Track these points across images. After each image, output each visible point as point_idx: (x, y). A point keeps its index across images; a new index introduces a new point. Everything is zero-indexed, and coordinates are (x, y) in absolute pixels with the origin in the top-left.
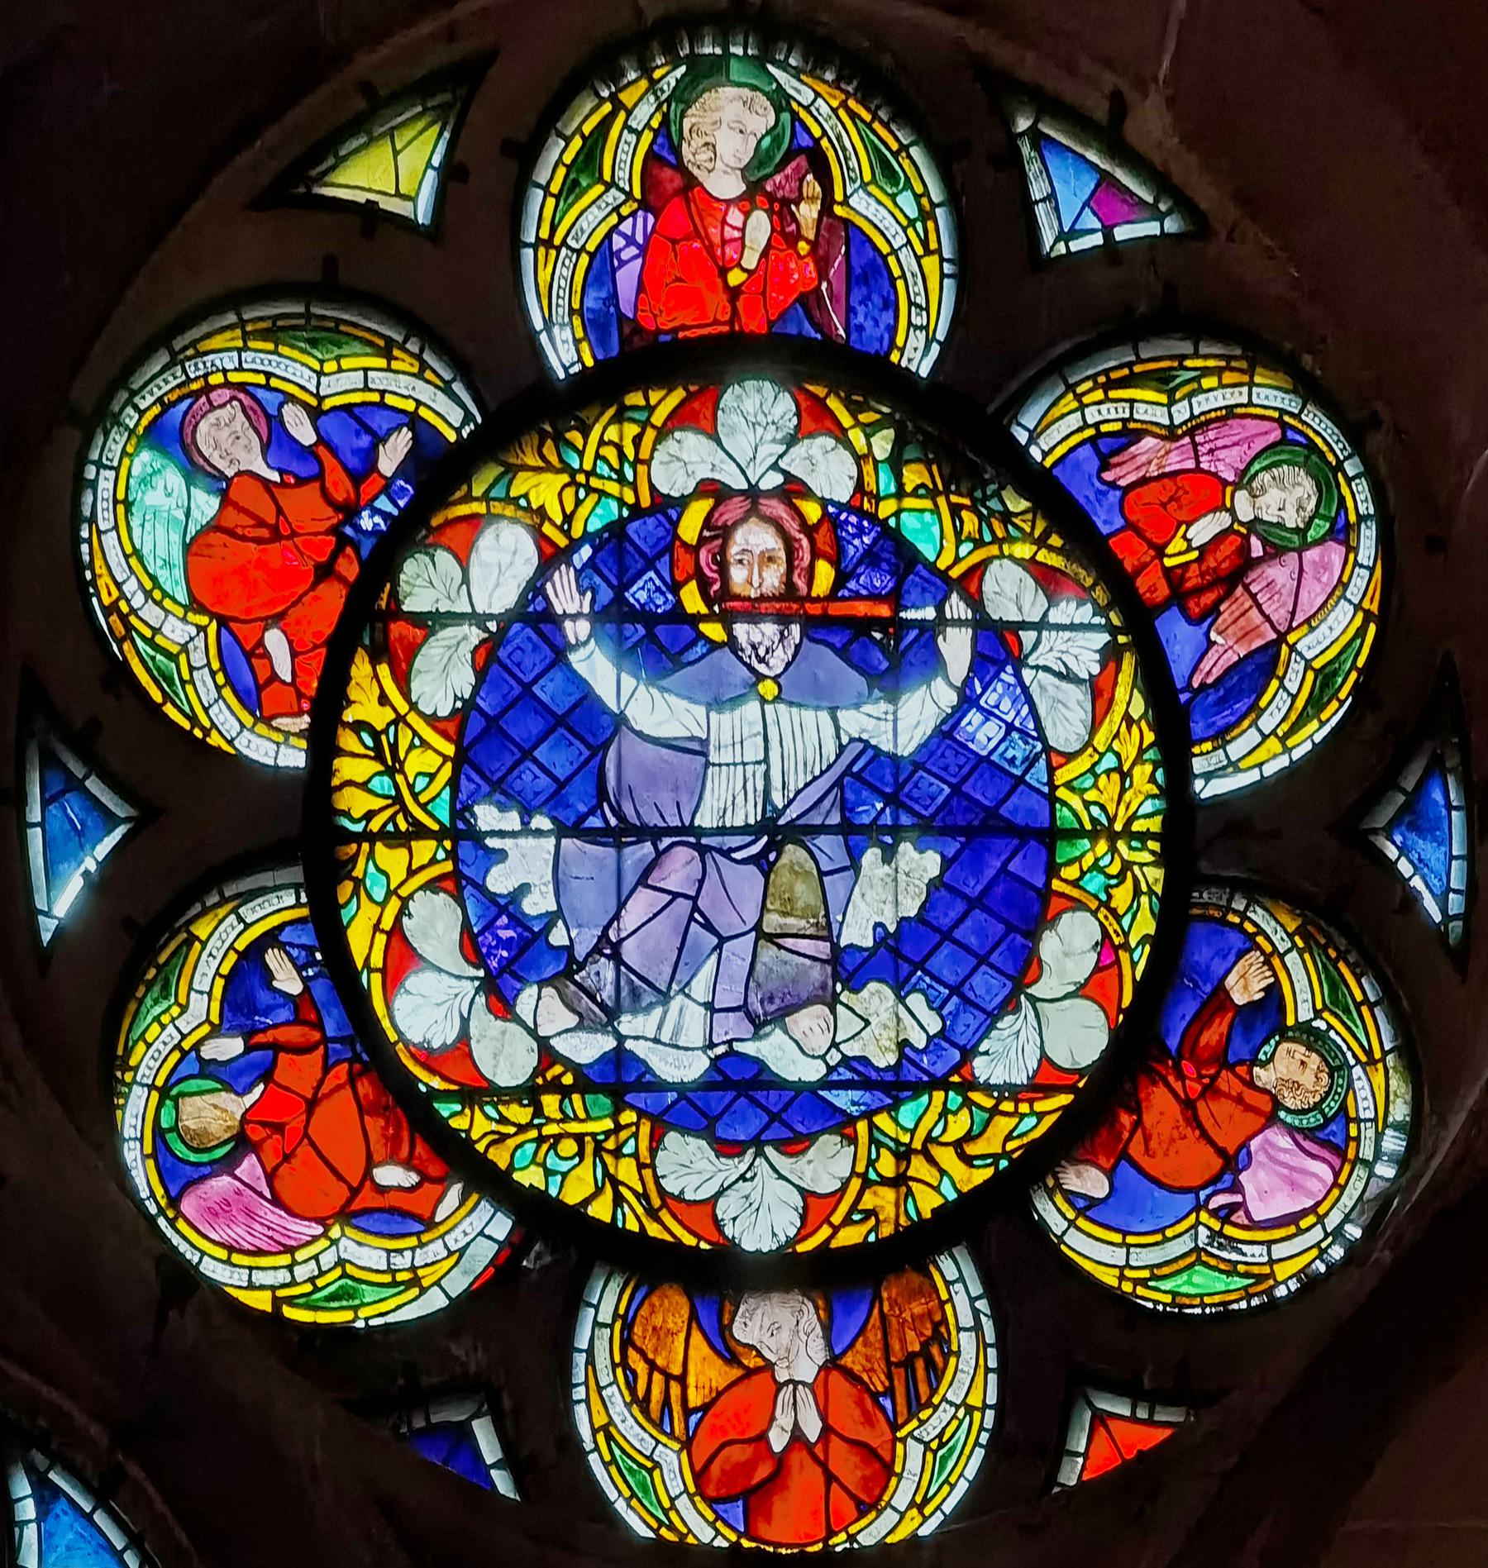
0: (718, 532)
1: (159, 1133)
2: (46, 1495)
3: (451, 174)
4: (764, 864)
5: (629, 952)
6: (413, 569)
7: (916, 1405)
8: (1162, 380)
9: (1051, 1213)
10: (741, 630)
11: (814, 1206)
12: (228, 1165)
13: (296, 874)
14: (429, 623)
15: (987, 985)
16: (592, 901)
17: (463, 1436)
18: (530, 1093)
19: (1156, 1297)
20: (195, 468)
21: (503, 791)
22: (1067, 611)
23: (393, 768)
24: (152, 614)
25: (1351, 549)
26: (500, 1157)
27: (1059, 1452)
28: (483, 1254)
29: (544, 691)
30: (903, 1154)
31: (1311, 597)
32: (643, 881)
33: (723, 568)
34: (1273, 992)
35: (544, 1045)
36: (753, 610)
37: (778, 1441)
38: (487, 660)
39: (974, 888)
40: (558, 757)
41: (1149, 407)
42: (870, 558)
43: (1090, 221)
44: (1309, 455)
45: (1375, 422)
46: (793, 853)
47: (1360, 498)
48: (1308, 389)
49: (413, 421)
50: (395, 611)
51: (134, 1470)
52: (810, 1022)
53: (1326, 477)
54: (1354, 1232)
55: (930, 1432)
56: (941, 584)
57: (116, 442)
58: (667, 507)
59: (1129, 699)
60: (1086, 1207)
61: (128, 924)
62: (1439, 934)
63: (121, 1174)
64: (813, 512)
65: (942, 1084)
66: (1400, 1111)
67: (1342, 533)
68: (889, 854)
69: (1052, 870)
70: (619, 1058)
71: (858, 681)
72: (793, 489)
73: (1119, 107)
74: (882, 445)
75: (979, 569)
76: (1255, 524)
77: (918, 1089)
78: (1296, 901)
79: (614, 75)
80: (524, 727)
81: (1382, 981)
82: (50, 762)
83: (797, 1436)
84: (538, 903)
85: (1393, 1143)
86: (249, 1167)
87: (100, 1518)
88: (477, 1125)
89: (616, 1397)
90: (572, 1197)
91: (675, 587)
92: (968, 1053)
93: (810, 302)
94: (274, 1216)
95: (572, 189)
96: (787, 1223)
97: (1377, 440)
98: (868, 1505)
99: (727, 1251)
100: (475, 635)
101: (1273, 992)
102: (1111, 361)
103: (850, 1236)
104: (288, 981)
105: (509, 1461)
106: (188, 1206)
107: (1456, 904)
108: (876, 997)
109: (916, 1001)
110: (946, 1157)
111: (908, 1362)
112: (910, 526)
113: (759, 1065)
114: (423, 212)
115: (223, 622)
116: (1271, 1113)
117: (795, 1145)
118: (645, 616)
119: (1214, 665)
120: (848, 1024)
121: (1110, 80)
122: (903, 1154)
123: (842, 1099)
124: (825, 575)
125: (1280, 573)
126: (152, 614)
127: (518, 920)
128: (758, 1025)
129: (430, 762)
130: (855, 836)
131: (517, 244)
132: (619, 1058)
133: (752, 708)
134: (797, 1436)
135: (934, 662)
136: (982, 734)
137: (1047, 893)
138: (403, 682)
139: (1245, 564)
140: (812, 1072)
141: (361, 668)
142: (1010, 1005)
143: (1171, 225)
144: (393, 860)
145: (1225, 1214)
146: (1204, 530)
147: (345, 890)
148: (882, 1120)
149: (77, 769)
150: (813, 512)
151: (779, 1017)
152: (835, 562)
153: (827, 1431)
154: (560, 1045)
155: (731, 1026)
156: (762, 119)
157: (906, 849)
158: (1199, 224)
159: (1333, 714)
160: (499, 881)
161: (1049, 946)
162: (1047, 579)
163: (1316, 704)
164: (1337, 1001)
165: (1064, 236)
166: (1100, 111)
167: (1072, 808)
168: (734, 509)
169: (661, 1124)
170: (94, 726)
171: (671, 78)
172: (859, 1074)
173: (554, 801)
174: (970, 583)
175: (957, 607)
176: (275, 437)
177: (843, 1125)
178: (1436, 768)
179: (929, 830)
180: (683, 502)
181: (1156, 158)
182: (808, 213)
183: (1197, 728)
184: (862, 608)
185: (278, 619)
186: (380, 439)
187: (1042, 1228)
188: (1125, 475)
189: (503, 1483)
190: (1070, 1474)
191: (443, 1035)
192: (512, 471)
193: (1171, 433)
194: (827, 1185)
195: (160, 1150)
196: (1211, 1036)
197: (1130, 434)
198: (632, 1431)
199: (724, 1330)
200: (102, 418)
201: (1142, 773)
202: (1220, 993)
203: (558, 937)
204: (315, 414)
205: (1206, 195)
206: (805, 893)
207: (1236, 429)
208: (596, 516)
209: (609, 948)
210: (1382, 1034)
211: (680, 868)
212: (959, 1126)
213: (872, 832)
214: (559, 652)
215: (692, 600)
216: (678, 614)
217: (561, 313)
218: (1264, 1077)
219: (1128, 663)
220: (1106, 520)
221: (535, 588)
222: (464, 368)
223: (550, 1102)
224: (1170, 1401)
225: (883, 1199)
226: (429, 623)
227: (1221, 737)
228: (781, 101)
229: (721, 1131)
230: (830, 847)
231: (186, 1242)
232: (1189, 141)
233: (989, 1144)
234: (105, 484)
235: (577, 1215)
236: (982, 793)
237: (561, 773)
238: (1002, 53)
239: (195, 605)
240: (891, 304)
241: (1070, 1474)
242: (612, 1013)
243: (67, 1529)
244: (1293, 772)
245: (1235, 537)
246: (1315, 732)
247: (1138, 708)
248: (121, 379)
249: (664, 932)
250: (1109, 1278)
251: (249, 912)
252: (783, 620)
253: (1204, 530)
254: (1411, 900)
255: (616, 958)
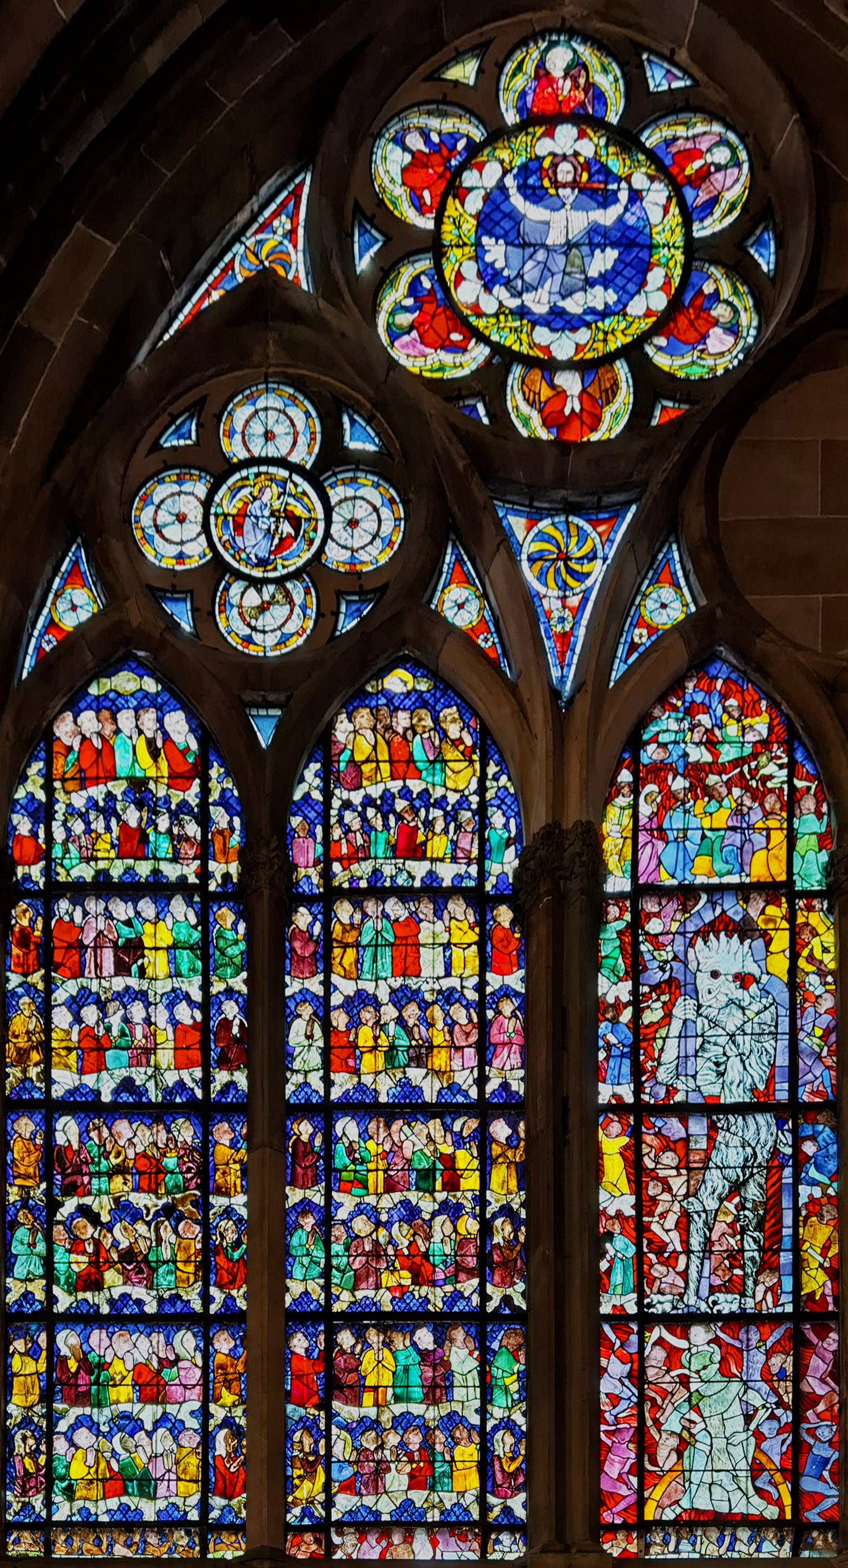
0: (554, 166)
1: (388, 325)
2: (353, 422)
3: (480, 71)
4: (566, 254)
5: (526, 277)
6: (466, 175)
7: (608, 402)
8: (685, 124)
9: (650, 350)
10: (561, 191)
11: (579, 348)
12: (409, 333)
13: (430, 255)
14: (470, 190)
15: (631, 287)
16: (516, 263)
17: (474, 408)
18: (496, 315)
19: (681, 374)
20: (405, 149)
21: (491, 234)
22: (657, 186)
23: (459, 227)
24: (391, 186)
25: (740, 170)
26: (487, 333)
27: (651, 416)
28: (481, 359)
29: (502, 207)
30: (606, 333)
31: (729, 183)
32: (531, 257)
33: (555, 174)
34: (717, 291)
35: (500, 303)
36: (564, 186)
37: (567, 411)
38: (487, 198)
39: (628, 260)
40: (507, 224)
41: (681, 131)
42: (598, 172)
43: (664, 82)
44: (728, 144)
45: (747, 135)
46: (574, 251)
47: (743, 155)
48: (728, 126)
49: (467, 136)
50: (460, 186)
51: (379, 415)
52: (579, 296)
53: (733, 150)
54: (741, 356)
55: (613, 410)
56: (619, 179)
57: (383, 141)
58: (540, 159)
59: (674, 210)
60: (660, 349)
61: (382, 269)
62: (766, 275)
63: (378, 336)
64: (582, 160)
65: (618, 314)
66: (755, 323)
67: (738, 165)
68: (603, 251)
69: (651, 256)
70: (523, 306)
71: (595, 205)
72: (576, 154)
73: (673, 52)
74: (603, 141)
75: (630, 175)
76: (712, 163)
77: (609, 315)
78: (724, 265)
79: (527, 45)
80: (497, 216)
81: (749, 287)
82: (361, 226)
83: (573, 410)
84: (499, 265)
85: (753, 332)
86: (414, 334)
87: (368, 429)
88: (480, 323)
89: (519, 397)
90: (508, 344)
91: (541, 179)
92: (625, 306)
93: (582, 105)
94: (422, 347)
95: (514, 75)
96: (571, 352)
97: (750, 140)
98: (594, 429)
99: (552, 359)
100: (482, 192)
101: (717, 291)
102: (670, 119)
103: (589, 356)
104: (427, 284)
105: (488, 414)
106: (396, 344)
107: (772, 266)
108: (599, 289)
109: (610, 291)
110: (619, 334)
111: (606, 390)
112: (610, 164)
113: (563, 309)
114: (471, 82)
115: (412, 189)
116: (715, 323)
117: (574, 329)
118: (533, 187)
119: (699, 201)
120: (590, 297)
121: (671, 46)
122: (606, 333)
123: (588, 318)
124: (585, 176)
125: (719, 176)
126: (391, 186)
127: (493, 268)
128: (563, 298)
129: (469, 226)
130: (593, 246)
131: (498, 90)
132: (523, 306)
133: (563, 211)
134: (573, 410)
135: (616, 201)
136: (631, 220)
137: (649, 263)
138: (462, 204)
139: (709, 174)
140: (579, 311)
141: (450, 200)
142: (638, 292)
143: (689, 83)
144: (458, 252)
145: (702, 351)
146: (697, 164)
147: (444, 260)
148: (600, 324)
149: (368, 227)
150: (582, 160)
151: (571, 294)
152: (589, 172)
153: (582, 409)
154: (505, 303)
155: (556, 298)
156: (570, 55)
157: (608, 249)
158: (696, 83)
159: (736, 214)
160: (488, 258)
161: (650, 276)
162: (652, 179)
163: (730, 212)
164: (736, 292)
165: (657, 86)
166: (667, 52)
167: (658, 239)
168: (557, 160)
169: (534, 324)
170: (374, 216)
171: (543, 45)
172: (592, 311)
173: (505, 236)
174: (628, 179)
175: (624, 185)
176: (427, 140)
177: (588, 325)
178: (766, 229)
179: (613, 245)
180: (544, 158)
181: (682, 64)
182: (582, 81)
183: (695, 216)
184: (595, 185)
185: (427, 188)
186: (457, 141)
187: (647, 355)
188: (674, 150)
189: (486, 421)
190: (654, 422)
191: (471, 300)
192: (495, 149)
193: (687, 139)
194: (582, 342)
195: (389, 327)
196: (698, 302)
197: (675, 139)
198: (525, 408)
199: (552, 380)
200: (380, 135)
201: (678, 229)
202: (700, 291)
203: (506, 273)
204: (440, 134)
205: (699, 75)
206: (578, 262)
207: (706, 137)
208: (518, 161)
209: (520, 276)
210: (750, 303)
211: (541, 255)
212: (623, 325)
213: (598, 245)
214: (507, 197)
215: (546, 183)
216: (542, 187)
217: (511, 105)
218: (714, 313)
219: (674, 201)
220: (668, 161)
221: (501, 179)
222: (481, 121)
223: (502, 318)
224: (685, 402)
225: (600, 345)
226: (470, 190)
227: (702, 220)
228: (575, 51)
229: (553, 325)
230: (586, 250)
231: (394, 354)
232: (693, 60)
233: (631, 331)
234: (379, 152)
235: (509, 349)
236: (632, 235)
237: (507, 228)
238: (640, 38)
239: (404, 184)
240: (606, 104)
241: (654, 422)
242: (520, 295)
243: (358, 430)
244: (723, 231)
245: (707, 166)
246: (730, 219)
247: (677, 211)
248: (386, 125)
249: (536, 273)
250: (667, 369)
251: (417, 265)
252: (573, 189)
253: (697, 164)
254: (759, 265)
255: (522, 278)
